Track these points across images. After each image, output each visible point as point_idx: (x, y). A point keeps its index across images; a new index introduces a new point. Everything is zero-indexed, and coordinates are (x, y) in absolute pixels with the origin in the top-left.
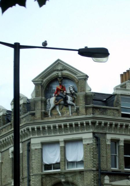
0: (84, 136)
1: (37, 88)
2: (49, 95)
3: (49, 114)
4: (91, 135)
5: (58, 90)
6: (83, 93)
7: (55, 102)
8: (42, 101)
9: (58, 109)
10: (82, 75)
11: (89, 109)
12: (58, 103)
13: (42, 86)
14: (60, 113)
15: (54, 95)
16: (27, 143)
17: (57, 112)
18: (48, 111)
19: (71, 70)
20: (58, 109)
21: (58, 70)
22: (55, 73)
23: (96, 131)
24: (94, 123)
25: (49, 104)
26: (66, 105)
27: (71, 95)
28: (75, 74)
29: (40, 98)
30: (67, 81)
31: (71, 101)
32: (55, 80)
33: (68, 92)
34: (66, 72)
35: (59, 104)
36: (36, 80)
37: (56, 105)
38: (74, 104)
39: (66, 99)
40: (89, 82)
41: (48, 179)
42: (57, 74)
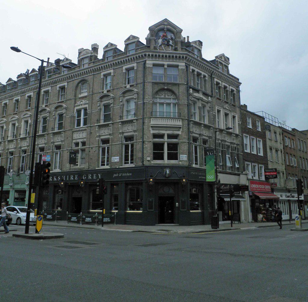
0: (180, 64)
4: (184, 64)
9: (163, 46)
15: (161, 38)
16: (143, 63)
20: (163, 46)
21: (164, 25)
24: (186, 57)
26: (168, 45)
28: (175, 29)
32: (162, 30)
33: (170, 38)
34: (169, 27)
35: (164, 44)
36: (152, 27)
38: (173, 45)
39: (168, 42)
41: (156, 86)
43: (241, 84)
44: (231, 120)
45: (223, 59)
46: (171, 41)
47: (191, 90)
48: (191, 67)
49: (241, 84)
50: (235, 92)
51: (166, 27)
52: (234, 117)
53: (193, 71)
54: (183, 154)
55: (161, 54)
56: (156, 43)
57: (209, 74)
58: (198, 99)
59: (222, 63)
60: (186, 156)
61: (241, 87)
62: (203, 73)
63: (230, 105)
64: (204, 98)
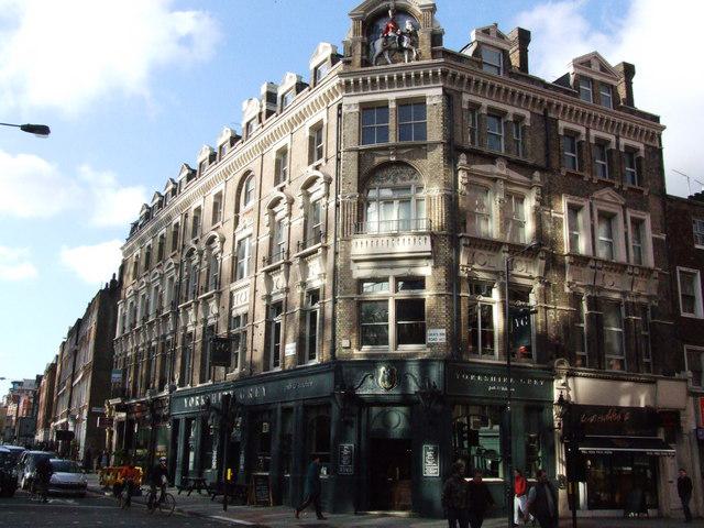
0: (428, 93)
2: (373, 36)
4: (440, 91)
8: (363, 44)
20: (387, 57)
24: (444, 74)
37: (385, 50)
43: (663, 128)
44: (626, 234)
45: (595, 67)
47: (463, 156)
48: (466, 98)
49: (663, 128)
50: (642, 154)
52: (637, 223)
53: (474, 107)
54: (435, 326)
57: (536, 111)
58: (495, 180)
59: (592, 80)
60: (444, 331)
61: (665, 136)
62: (511, 110)
63: (619, 191)
64: (515, 175)
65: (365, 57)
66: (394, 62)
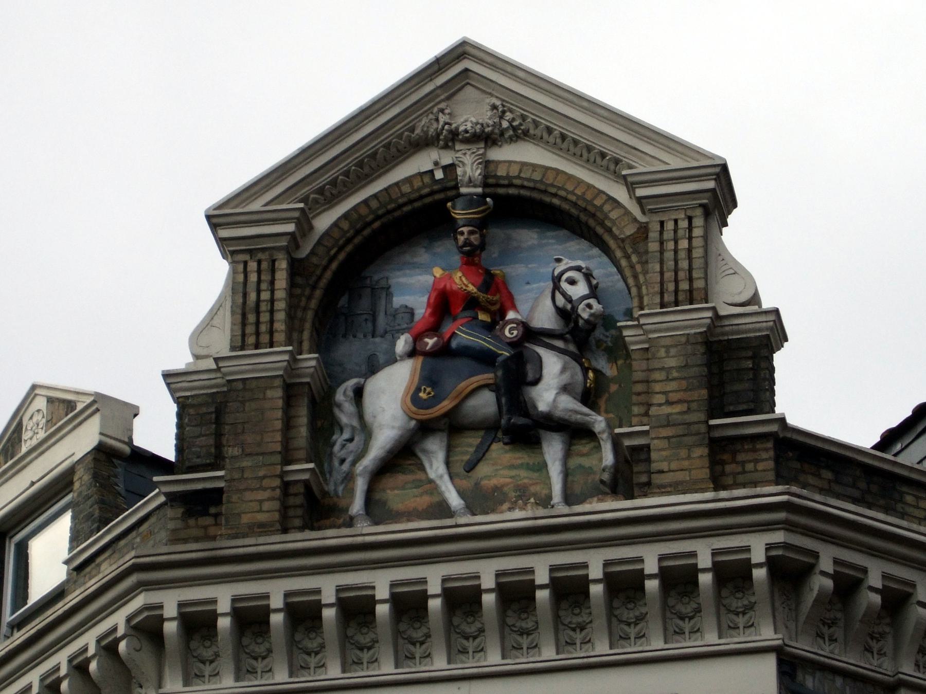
1: (253, 278)
2: (351, 350)
3: (357, 506)
5: (444, 304)
6: (693, 319)
7: (415, 399)
8: (291, 391)
10: (675, 162)
11: (741, 457)
12: (446, 405)
13: (297, 268)
14: (454, 500)
15: (402, 344)
17: (432, 486)
18: (349, 478)
19: (573, 132)
21: (452, 139)
22: (428, 166)
23: (804, 647)
24: (788, 573)
25: (355, 423)
26: (524, 429)
27: (572, 348)
29: (274, 359)
30: (527, 237)
31: (565, 389)
32: (419, 219)
33: (544, 317)
34: (522, 155)
35: (452, 426)
36: (256, 206)
38: (599, 423)
39: (517, 376)
40: (738, 237)
42: (439, 175)
46: (553, 365)
51: (469, 167)
55: (382, 583)
56: (324, 422)
65: (302, 469)
66: (479, 500)
